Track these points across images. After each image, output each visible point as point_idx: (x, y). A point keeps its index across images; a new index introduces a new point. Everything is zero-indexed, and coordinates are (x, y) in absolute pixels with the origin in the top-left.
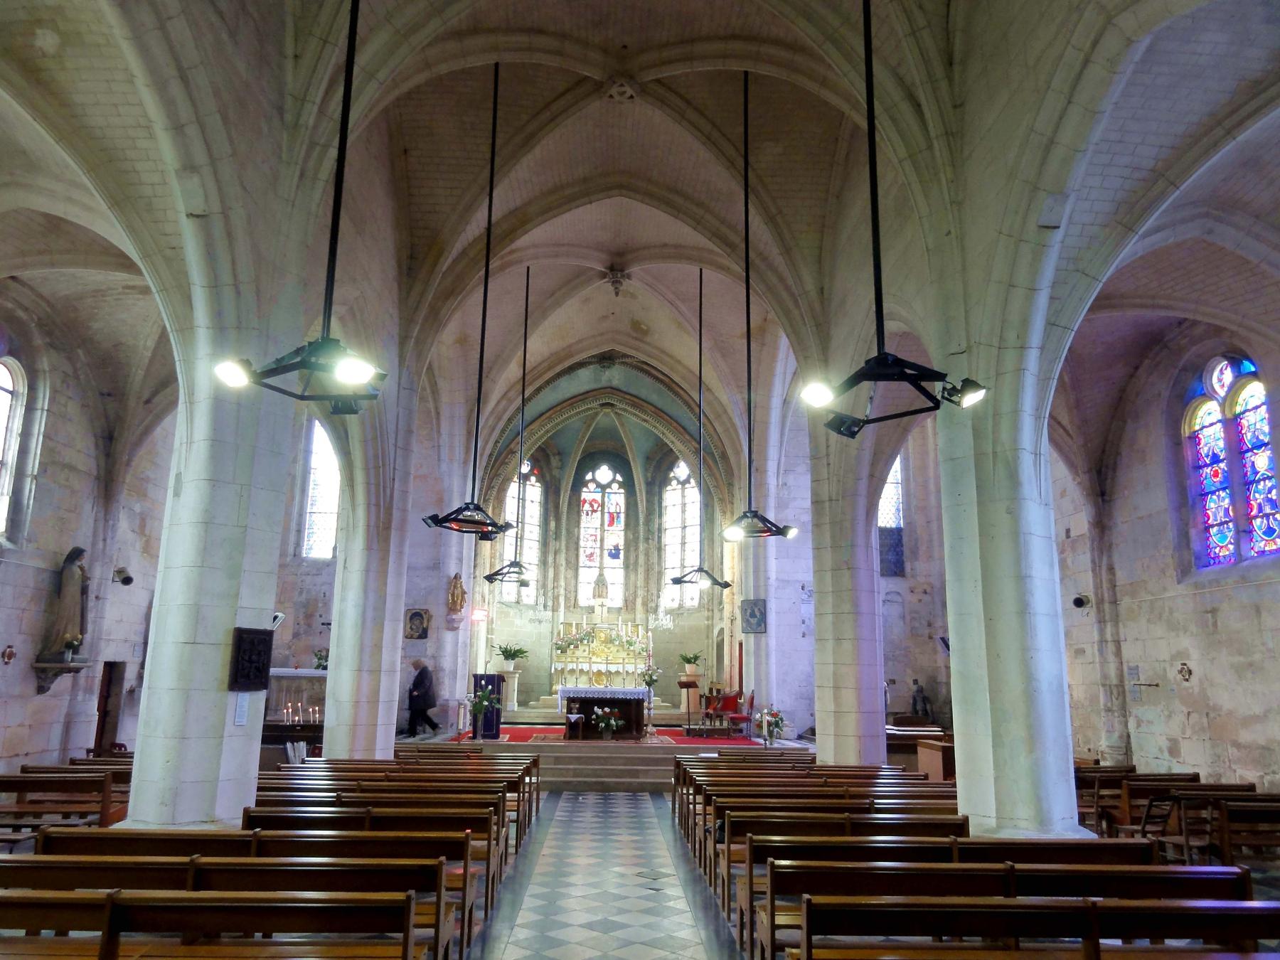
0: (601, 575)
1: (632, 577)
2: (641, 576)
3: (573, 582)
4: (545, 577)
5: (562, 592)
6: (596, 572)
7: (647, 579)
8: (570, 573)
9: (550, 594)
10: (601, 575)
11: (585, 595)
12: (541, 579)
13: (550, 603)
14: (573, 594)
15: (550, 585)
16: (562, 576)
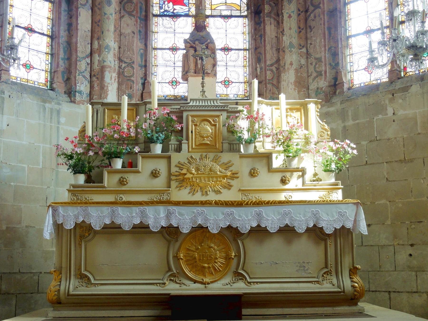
0: (200, 27)
1: (270, 29)
2: (290, 23)
3: (137, 45)
4: (71, 28)
5: (110, 59)
6: (186, 27)
7: (305, 28)
8: (130, 25)
9: (83, 65)
10: (200, 27)
11: (167, 78)
12: (63, 33)
13: (83, 86)
14: (139, 73)
15: (83, 47)
16: (110, 26)
